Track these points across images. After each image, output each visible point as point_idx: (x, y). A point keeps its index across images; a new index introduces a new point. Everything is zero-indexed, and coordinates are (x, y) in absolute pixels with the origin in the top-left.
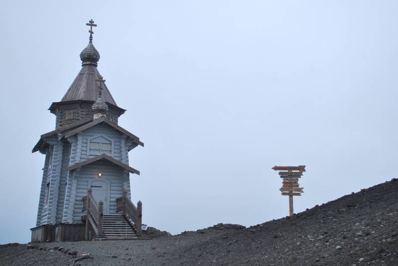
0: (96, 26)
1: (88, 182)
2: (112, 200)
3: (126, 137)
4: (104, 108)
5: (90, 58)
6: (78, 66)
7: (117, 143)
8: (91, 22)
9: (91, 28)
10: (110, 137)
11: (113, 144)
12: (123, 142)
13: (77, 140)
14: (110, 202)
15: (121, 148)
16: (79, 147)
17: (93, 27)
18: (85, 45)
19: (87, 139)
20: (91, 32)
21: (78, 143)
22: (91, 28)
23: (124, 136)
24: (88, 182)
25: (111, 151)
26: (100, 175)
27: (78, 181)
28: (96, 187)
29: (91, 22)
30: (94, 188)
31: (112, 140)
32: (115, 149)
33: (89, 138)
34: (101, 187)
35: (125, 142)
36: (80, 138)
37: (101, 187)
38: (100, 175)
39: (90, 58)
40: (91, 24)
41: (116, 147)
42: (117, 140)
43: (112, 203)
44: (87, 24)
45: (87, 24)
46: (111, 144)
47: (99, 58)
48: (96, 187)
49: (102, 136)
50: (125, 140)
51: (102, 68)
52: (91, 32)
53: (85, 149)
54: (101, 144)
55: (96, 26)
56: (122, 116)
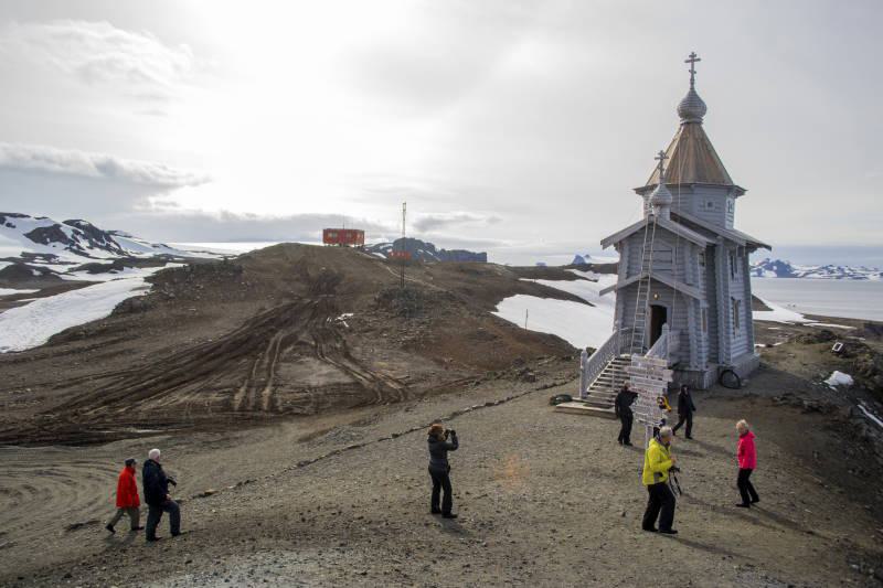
0: (699, 60)
5: (692, 111)
6: (673, 126)
8: (693, 56)
12: (688, 248)
18: (684, 93)
20: (693, 72)
29: (693, 56)
36: (626, 248)
39: (692, 111)
40: (693, 59)
44: (687, 62)
45: (687, 62)
51: (709, 125)
52: (693, 72)
55: (699, 60)
56: (740, 198)
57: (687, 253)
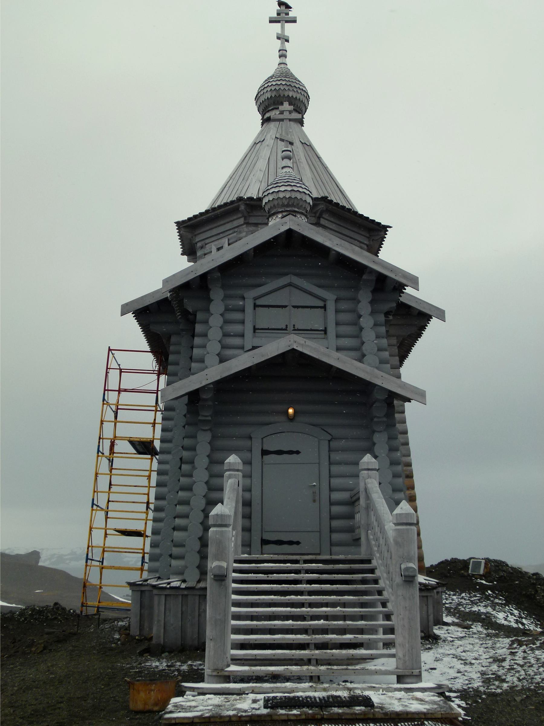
1: (250, 438)
2: (337, 496)
3: (374, 278)
4: (299, 196)
7: (343, 306)
9: (283, 28)
10: (320, 286)
11: (331, 306)
13: (210, 300)
14: (331, 504)
15: (360, 316)
16: (216, 321)
17: (287, 25)
19: (243, 298)
20: (283, 38)
21: (213, 307)
22: (283, 28)
23: (365, 277)
24: (250, 438)
25: (325, 331)
26: (291, 411)
27: (214, 437)
28: (279, 452)
30: (273, 456)
31: (330, 296)
32: (337, 324)
33: (251, 294)
34: (298, 452)
35: (369, 296)
37: (298, 452)
38: (291, 411)
41: (343, 317)
42: (344, 293)
43: (336, 509)
45: (272, 21)
46: (324, 307)
47: (308, 98)
48: (279, 452)
49: (290, 285)
50: (374, 291)
52: (283, 38)
53: (238, 328)
54: (292, 307)
57: (365, 308)
